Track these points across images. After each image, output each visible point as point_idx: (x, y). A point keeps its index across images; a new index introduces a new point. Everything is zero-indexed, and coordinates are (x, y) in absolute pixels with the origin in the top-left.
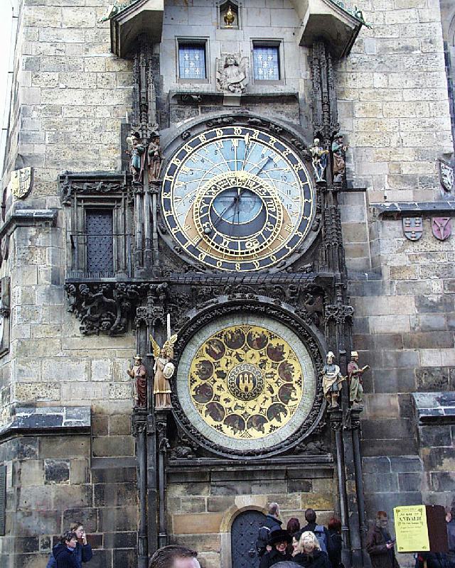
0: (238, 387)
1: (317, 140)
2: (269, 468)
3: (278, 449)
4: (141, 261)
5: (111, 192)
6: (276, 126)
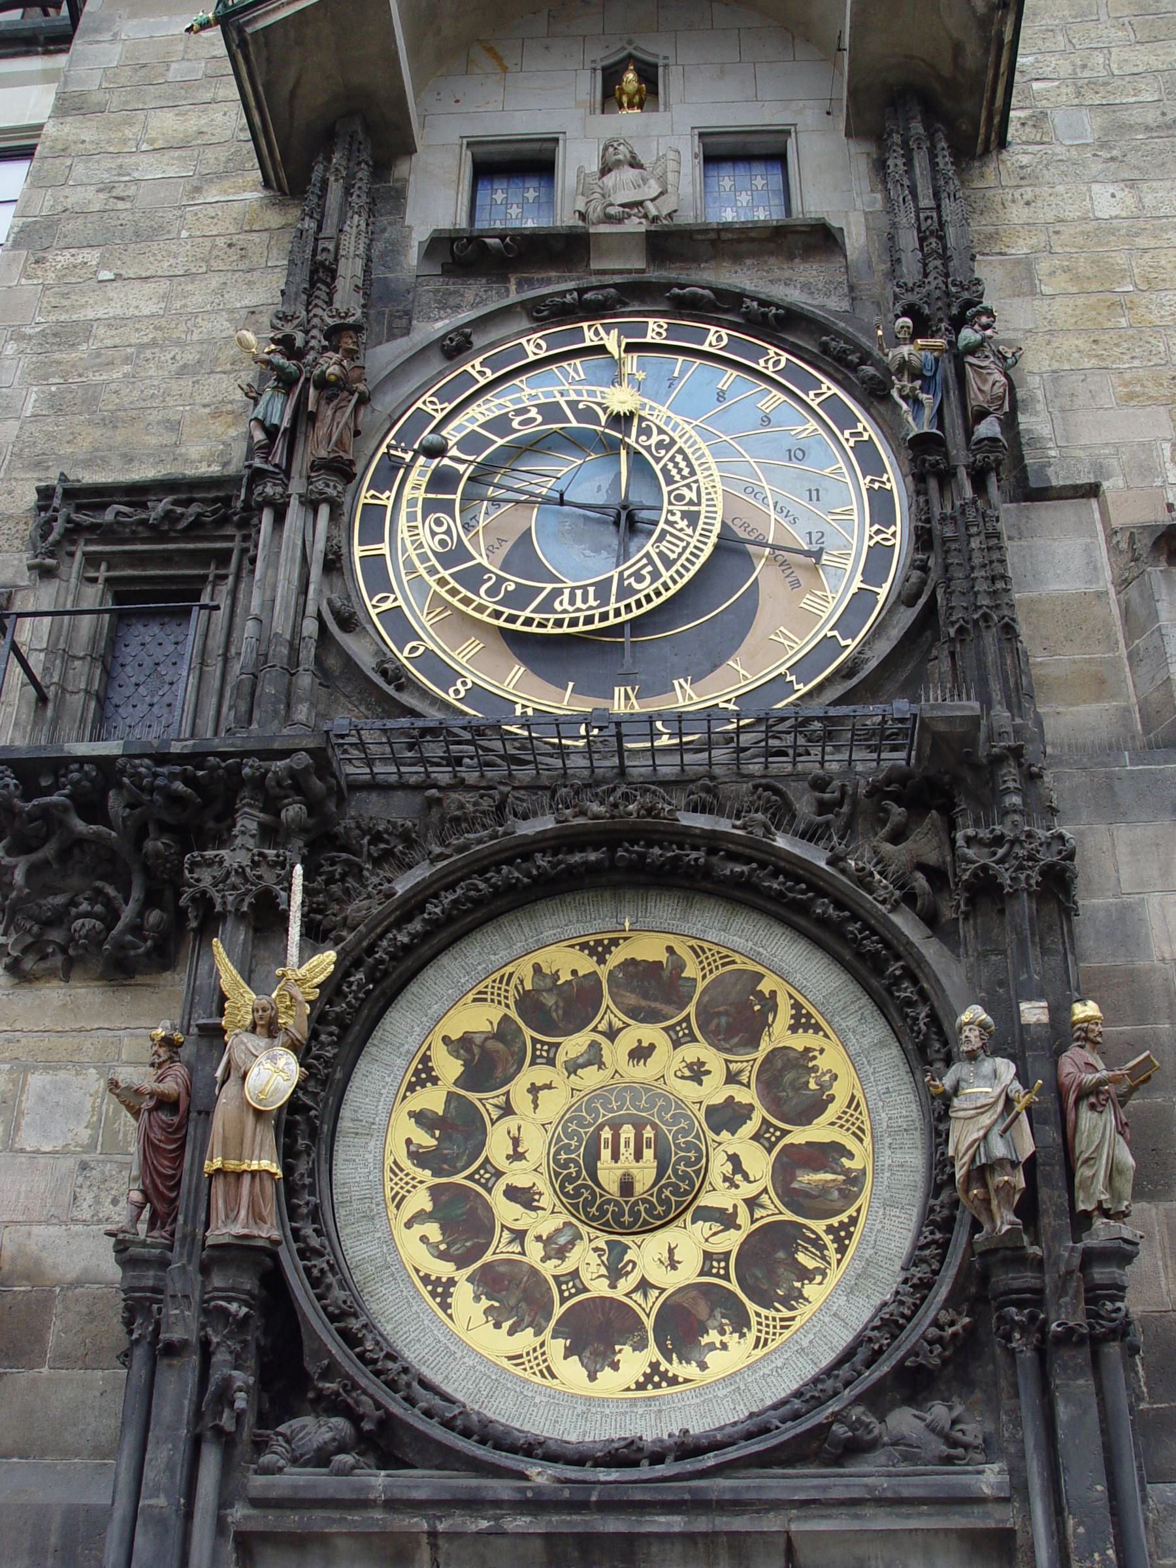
0: (594, 1176)
1: (907, 321)
2: (702, 1524)
3: (749, 1436)
4: (243, 707)
5: (196, 528)
6: (763, 303)
